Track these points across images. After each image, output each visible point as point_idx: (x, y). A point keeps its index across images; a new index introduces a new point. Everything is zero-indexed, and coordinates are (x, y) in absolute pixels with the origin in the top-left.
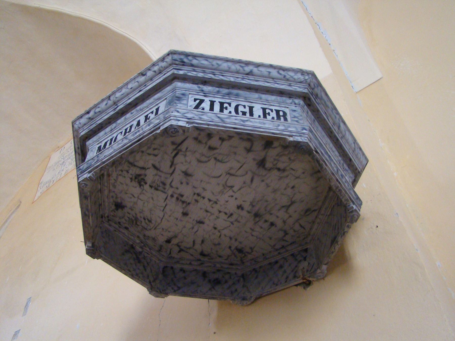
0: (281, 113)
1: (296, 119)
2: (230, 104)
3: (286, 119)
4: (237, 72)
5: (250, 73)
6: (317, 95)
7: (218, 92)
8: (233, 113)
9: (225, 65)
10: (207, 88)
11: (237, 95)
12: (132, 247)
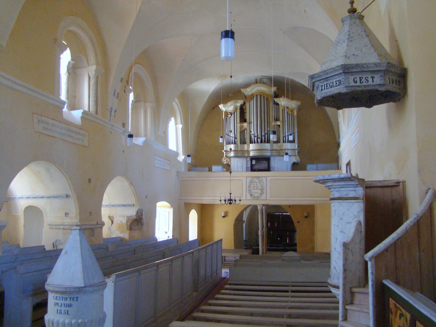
0: (340, 81)
1: (343, 83)
2: (328, 84)
3: (341, 85)
4: (325, 74)
5: (327, 73)
6: (347, 69)
7: (324, 81)
8: (329, 88)
9: (321, 74)
10: (322, 81)
11: (329, 80)
12: (354, 97)
